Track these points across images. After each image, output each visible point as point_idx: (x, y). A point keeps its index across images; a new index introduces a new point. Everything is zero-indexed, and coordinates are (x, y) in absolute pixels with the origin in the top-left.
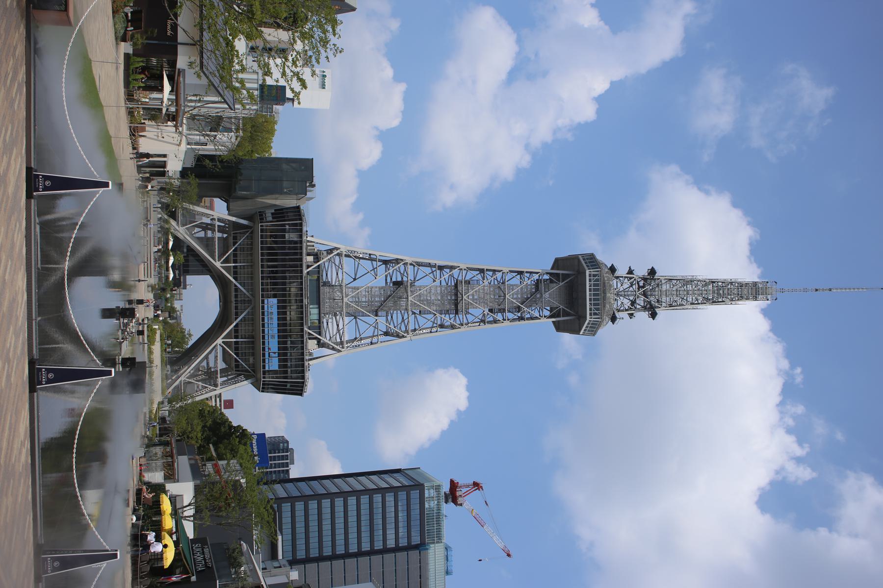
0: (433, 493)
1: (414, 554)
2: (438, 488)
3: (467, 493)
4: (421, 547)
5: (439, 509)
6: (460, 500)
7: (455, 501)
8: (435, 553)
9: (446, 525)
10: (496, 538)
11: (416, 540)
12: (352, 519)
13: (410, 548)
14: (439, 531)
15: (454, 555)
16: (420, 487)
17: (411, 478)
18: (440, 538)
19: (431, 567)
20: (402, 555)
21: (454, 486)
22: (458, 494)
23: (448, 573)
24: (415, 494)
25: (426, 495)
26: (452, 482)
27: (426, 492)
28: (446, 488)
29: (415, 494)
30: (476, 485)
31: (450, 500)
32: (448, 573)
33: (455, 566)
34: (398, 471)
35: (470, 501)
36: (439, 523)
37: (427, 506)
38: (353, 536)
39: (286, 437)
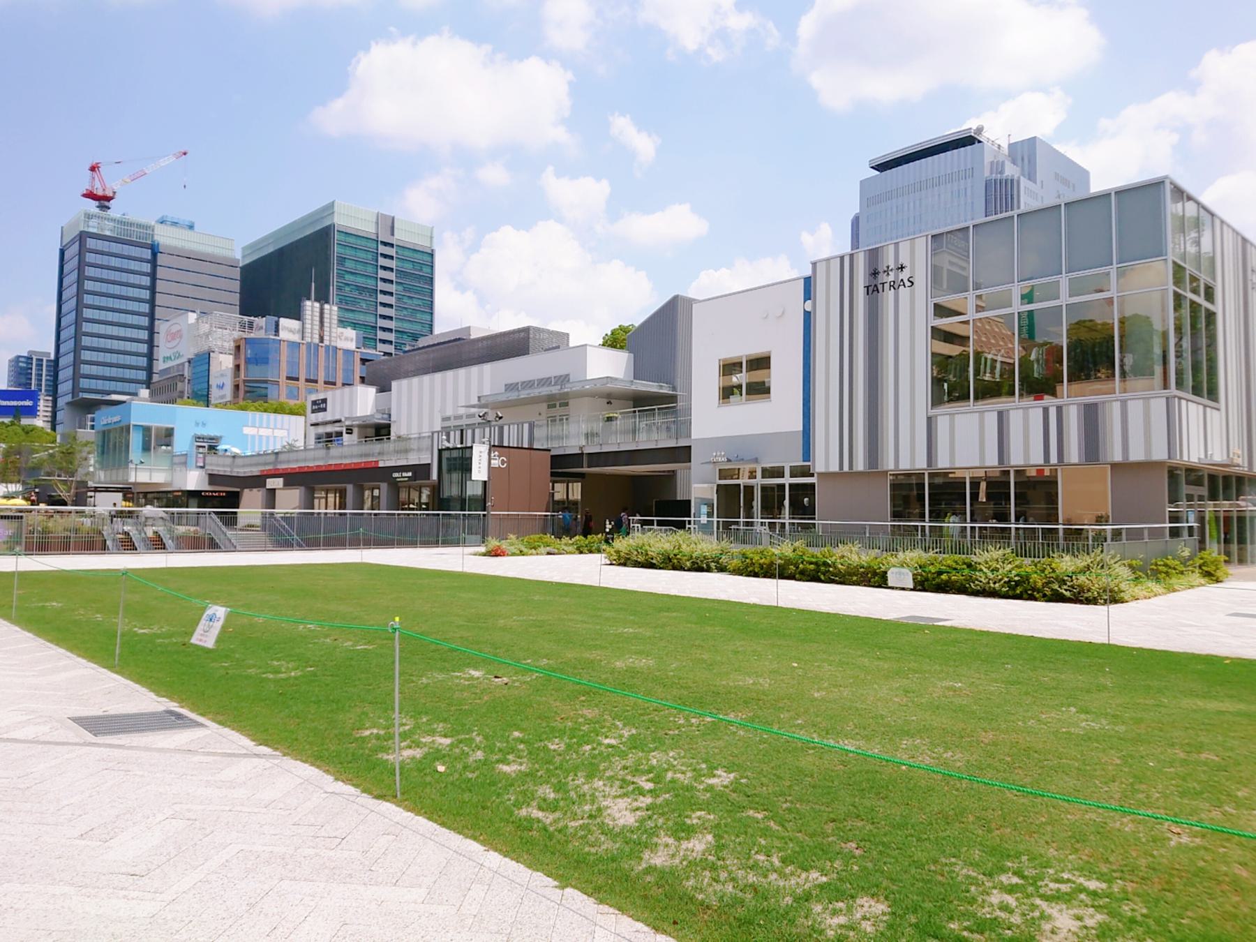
0: (93, 222)
1: (161, 259)
2: (89, 216)
3: (102, 181)
4: (155, 250)
5: (114, 220)
6: (110, 194)
7: (109, 199)
8: (165, 237)
9: (134, 217)
10: (164, 162)
11: (147, 254)
12: (110, 316)
13: (153, 262)
14: (139, 226)
15: (172, 215)
16: (83, 237)
17: (72, 242)
18: (146, 227)
19: (179, 244)
20: (161, 272)
21: (90, 195)
22: (100, 193)
23: (191, 227)
24: (91, 243)
25: (95, 231)
26: (85, 196)
27: (91, 230)
28: (92, 206)
29: (91, 243)
30: (93, 169)
31: (106, 203)
32: (191, 227)
33: (185, 218)
34: (62, 252)
35: (110, 181)
36: (131, 224)
37: (108, 233)
38: (130, 319)
39: (12, 356)
